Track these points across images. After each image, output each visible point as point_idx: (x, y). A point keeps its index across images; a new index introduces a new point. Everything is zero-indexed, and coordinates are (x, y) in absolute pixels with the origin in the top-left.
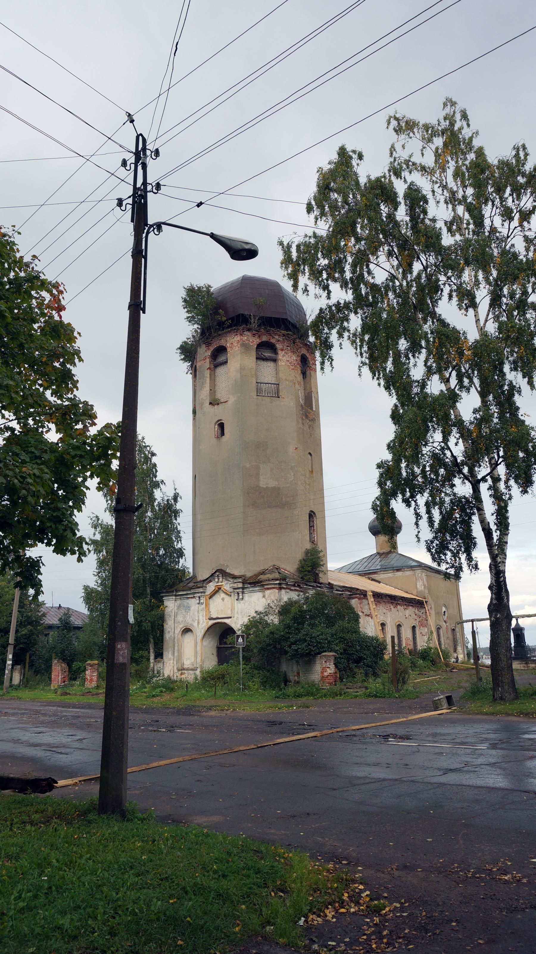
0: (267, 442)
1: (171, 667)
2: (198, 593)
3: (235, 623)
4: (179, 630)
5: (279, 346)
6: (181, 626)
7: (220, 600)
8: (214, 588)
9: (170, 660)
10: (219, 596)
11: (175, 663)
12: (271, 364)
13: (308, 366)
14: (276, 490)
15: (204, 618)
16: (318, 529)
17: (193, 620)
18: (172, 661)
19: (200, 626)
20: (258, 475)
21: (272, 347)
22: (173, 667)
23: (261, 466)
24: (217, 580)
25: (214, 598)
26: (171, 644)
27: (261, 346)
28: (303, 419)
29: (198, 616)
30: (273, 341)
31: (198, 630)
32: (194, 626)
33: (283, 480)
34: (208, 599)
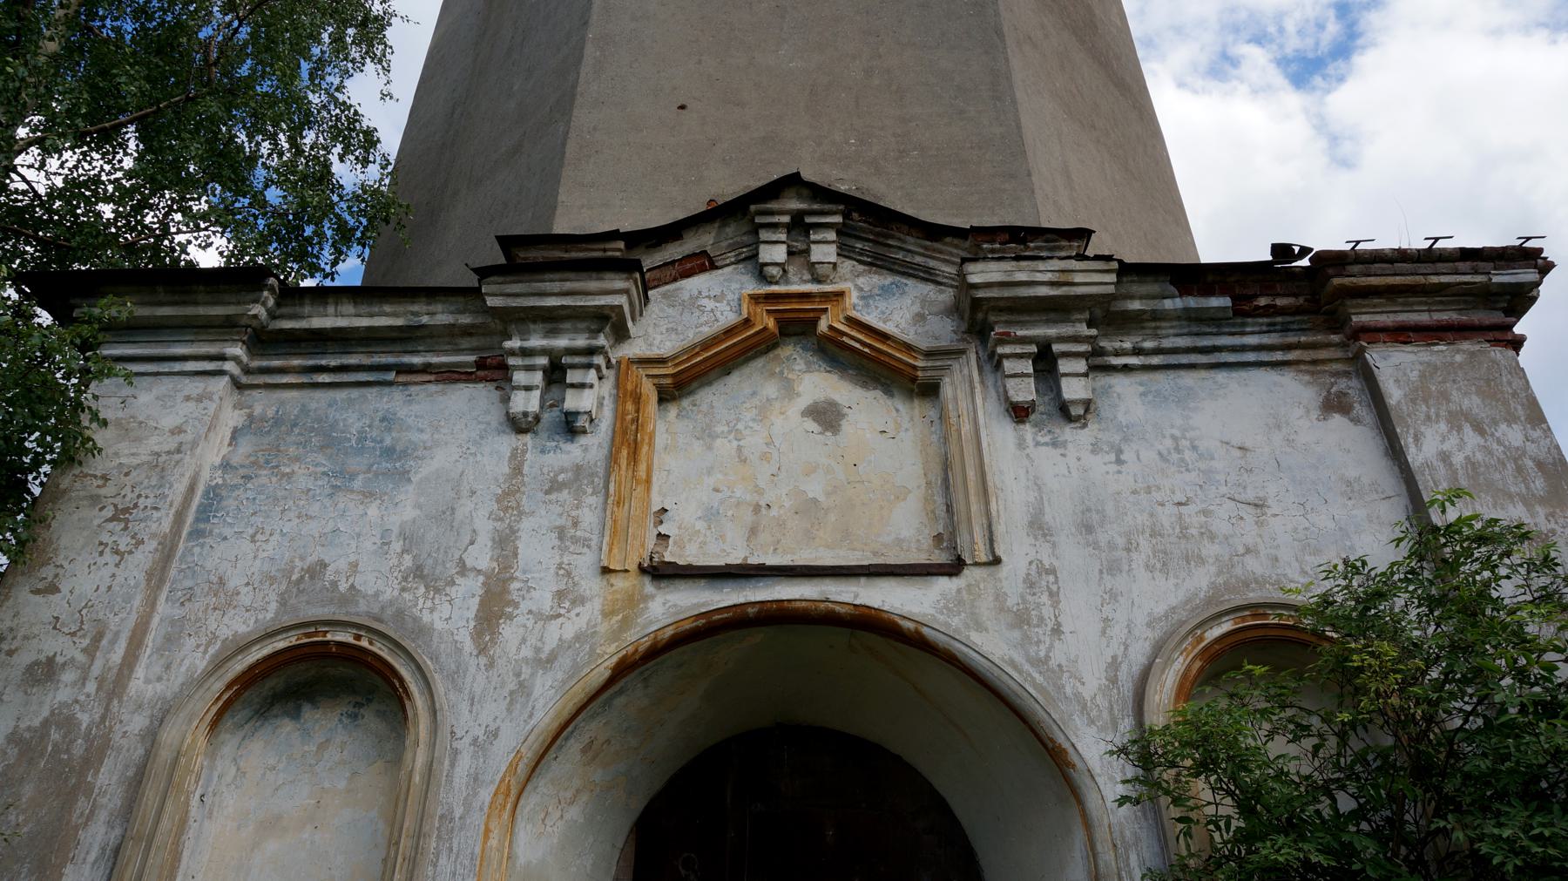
2: (551, 319)
3: (1021, 619)
4: (192, 657)
7: (789, 421)
8: (728, 317)
10: (771, 389)
15: (584, 563)
17: (418, 572)
19: (509, 632)
24: (775, 253)
25: (713, 399)
29: (505, 543)
31: (476, 678)
32: (423, 631)
34: (649, 390)
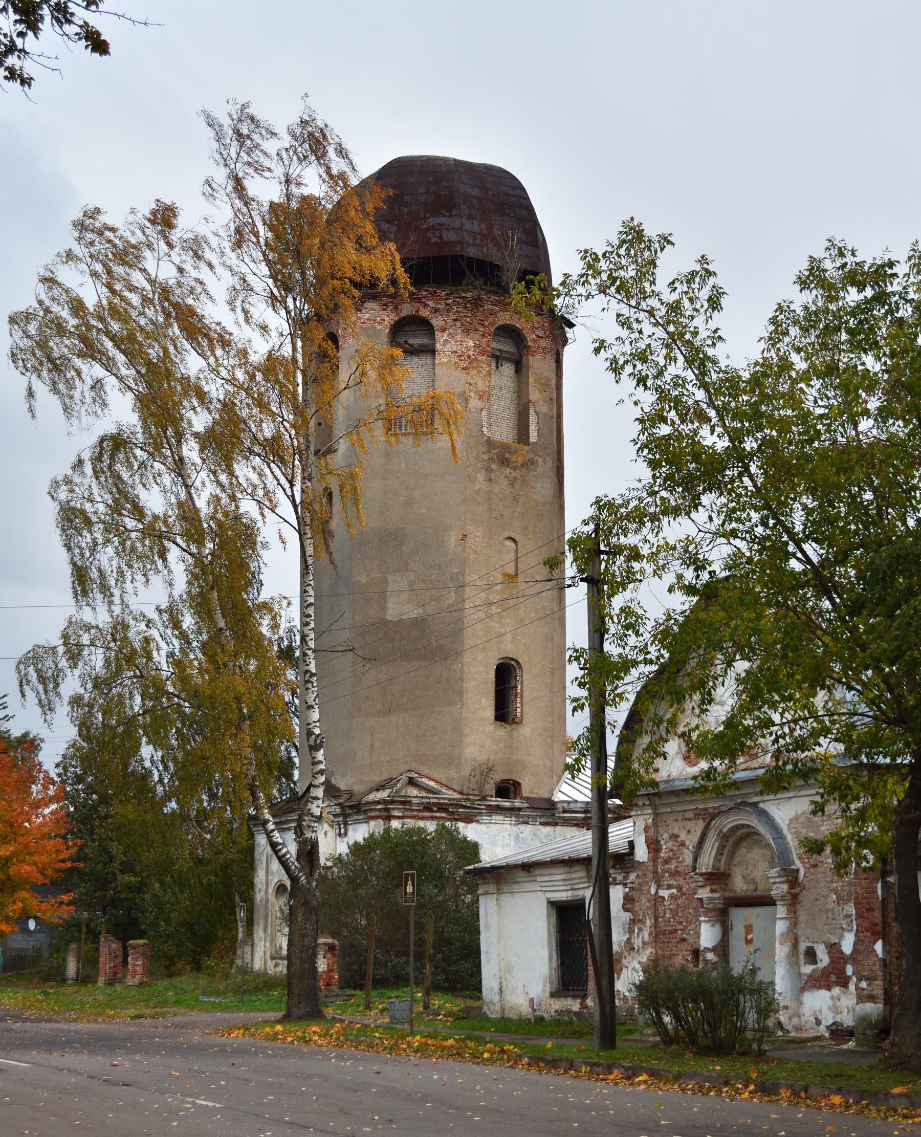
0: (404, 529)
1: (262, 953)
5: (437, 322)
6: (276, 880)
9: (261, 940)
11: (268, 945)
12: (425, 360)
13: (525, 346)
14: (419, 623)
16: (525, 694)
18: (263, 943)
20: (383, 596)
21: (426, 326)
22: (265, 952)
23: (390, 578)
26: (262, 912)
27: (398, 329)
28: (489, 470)
30: (424, 313)
33: (434, 603)
